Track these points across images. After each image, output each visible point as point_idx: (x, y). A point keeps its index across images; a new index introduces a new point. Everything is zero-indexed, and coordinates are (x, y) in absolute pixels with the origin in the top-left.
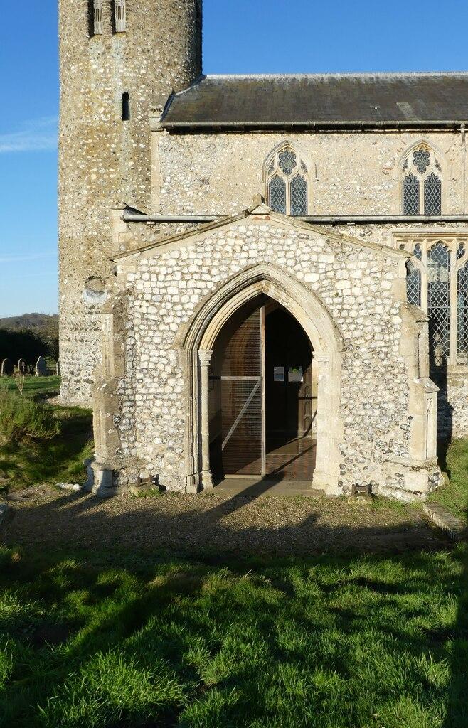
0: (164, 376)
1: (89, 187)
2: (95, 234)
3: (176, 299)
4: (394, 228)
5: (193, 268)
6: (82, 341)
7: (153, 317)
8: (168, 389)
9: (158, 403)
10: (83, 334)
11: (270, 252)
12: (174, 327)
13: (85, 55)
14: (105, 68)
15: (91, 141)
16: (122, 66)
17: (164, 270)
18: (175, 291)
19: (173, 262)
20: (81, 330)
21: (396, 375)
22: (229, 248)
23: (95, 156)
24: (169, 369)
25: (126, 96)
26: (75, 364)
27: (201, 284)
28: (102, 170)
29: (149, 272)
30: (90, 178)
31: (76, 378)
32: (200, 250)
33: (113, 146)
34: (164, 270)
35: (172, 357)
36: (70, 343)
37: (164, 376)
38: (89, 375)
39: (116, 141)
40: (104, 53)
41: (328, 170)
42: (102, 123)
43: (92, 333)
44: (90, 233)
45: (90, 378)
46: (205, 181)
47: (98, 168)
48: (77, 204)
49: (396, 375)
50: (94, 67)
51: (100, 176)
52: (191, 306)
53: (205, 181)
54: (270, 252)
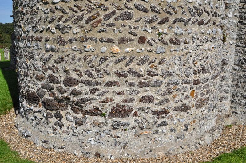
6: (175, 42)
10: (180, 29)
20: (174, 22)
26: (157, 84)
31: (159, 108)
36: (145, 47)
43: (195, 29)
45: (186, 102)
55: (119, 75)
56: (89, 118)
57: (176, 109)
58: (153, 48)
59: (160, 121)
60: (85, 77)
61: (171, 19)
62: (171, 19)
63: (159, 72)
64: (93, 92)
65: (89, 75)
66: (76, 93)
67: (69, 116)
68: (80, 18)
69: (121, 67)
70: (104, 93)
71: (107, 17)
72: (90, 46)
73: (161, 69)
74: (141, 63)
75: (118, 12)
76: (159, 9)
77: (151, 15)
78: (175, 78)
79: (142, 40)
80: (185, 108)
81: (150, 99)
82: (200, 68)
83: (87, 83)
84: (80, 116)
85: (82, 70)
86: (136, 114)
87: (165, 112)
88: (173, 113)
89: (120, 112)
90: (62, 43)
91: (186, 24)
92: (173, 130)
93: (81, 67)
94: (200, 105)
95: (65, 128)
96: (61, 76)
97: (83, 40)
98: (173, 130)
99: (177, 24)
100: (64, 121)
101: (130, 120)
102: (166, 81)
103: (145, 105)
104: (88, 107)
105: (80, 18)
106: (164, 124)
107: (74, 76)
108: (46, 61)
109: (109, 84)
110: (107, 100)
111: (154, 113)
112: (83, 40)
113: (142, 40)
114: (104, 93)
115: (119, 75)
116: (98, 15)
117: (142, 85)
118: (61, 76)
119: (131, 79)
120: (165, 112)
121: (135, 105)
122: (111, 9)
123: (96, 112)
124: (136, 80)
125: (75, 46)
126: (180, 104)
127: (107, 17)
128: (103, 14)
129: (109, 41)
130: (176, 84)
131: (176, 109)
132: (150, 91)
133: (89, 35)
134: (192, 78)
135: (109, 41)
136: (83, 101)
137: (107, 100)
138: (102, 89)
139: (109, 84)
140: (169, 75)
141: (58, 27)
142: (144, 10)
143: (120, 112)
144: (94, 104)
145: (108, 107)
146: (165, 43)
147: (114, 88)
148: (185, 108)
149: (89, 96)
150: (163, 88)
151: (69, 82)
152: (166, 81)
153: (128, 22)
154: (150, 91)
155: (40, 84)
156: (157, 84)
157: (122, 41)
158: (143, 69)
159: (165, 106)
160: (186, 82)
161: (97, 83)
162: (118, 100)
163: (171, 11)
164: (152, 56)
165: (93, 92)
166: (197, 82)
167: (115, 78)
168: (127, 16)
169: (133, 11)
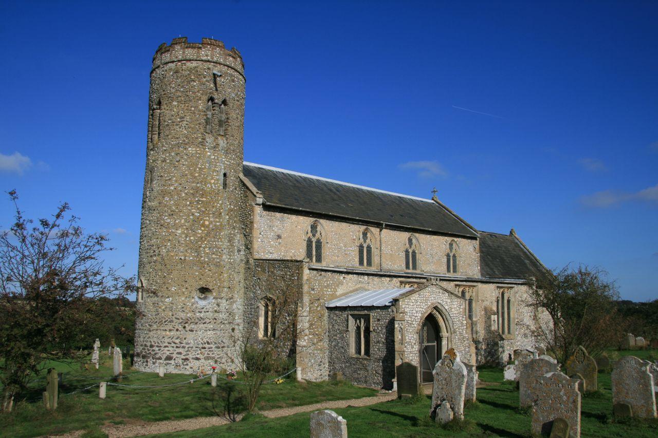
0: (413, 344)
1: (202, 229)
2: (207, 260)
3: (415, 315)
4: (400, 279)
5: (419, 303)
6: (192, 331)
7: (410, 322)
8: (414, 349)
9: (411, 355)
10: (193, 326)
11: (436, 298)
12: (415, 326)
13: (202, 145)
14: (215, 156)
15: (204, 199)
16: (223, 157)
17: (412, 304)
18: (414, 312)
19: (413, 301)
21: (465, 341)
22: (427, 296)
23: (208, 209)
24: (414, 342)
25: (225, 175)
27: (421, 310)
28: (212, 219)
29: (408, 304)
30: (204, 223)
31: (184, 357)
32: (420, 297)
33: (218, 205)
34: (412, 304)
35: (415, 337)
36: (178, 333)
37: (413, 344)
38: (198, 354)
39: (220, 202)
40: (215, 147)
41: (332, 237)
42: (213, 189)
44: (202, 259)
45: (198, 356)
46: (279, 237)
47: (209, 217)
48: (192, 238)
49: (465, 341)
50: (209, 154)
51: (211, 223)
52: (419, 317)
53: (279, 237)
54: (436, 298)
55: (169, 343)
56: (158, 361)
57: (193, 358)
58: (182, 333)
59: (185, 363)
60: (157, 344)
61: (189, 322)
62: (189, 322)
63: (184, 342)
64: (159, 350)
65: (158, 343)
66: (153, 351)
67: (150, 361)
68: (156, 322)
69: (170, 340)
70: (163, 350)
71: (165, 322)
72: (159, 332)
73: (185, 341)
74: (177, 339)
75: (169, 320)
76: (184, 318)
77: (181, 321)
78: (191, 345)
79: (177, 330)
80: (198, 359)
81: (180, 353)
82: (205, 342)
83: (157, 346)
84: (154, 361)
85: (156, 341)
86: (175, 360)
87: (187, 359)
88: (192, 360)
89: (169, 358)
90: (150, 331)
91: (196, 323)
92: (191, 368)
93: (155, 340)
95: (148, 366)
96: (149, 344)
97: (157, 330)
98: (191, 368)
99: (192, 324)
100: (149, 364)
101: (172, 362)
102: (187, 346)
103: (179, 356)
104: (157, 356)
105: (156, 322)
106: (187, 365)
107: (153, 344)
108: (144, 338)
109: (165, 347)
110: (164, 353)
111: (182, 359)
112: (157, 330)
113: (177, 330)
114: (163, 350)
115: (169, 343)
116: (162, 321)
117: (177, 347)
118: (149, 344)
119: (173, 345)
120: (187, 359)
121: (174, 356)
122: (167, 319)
123: (160, 358)
124: (175, 345)
125: (154, 332)
126: (194, 356)
127: (165, 322)
128: (164, 321)
129: (166, 330)
130: (192, 347)
131: (193, 358)
132: (180, 350)
133: (159, 328)
134: (201, 346)
135: (166, 330)
136: (156, 354)
137: (164, 353)
138: (162, 349)
139: (165, 347)
140: (189, 344)
141: (149, 325)
142: (178, 319)
143: (169, 358)
144: (159, 355)
145: (165, 356)
146: (187, 331)
147: (167, 349)
148: (198, 359)
149: (158, 352)
150: (186, 349)
151: (152, 346)
152: (187, 346)
153: (172, 324)
154: (180, 350)
155: (142, 348)
156: (184, 347)
157: (170, 330)
158: (177, 341)
159: (187, 357)
160: (197, 347)
161: (161, 347)
162: (168, 353)
163: (189, 319)
164: (181, 336)
165: (159, 350)
166: (204, 348)
167: (167, 345)
168: (172, 321)
169: (174, 319)
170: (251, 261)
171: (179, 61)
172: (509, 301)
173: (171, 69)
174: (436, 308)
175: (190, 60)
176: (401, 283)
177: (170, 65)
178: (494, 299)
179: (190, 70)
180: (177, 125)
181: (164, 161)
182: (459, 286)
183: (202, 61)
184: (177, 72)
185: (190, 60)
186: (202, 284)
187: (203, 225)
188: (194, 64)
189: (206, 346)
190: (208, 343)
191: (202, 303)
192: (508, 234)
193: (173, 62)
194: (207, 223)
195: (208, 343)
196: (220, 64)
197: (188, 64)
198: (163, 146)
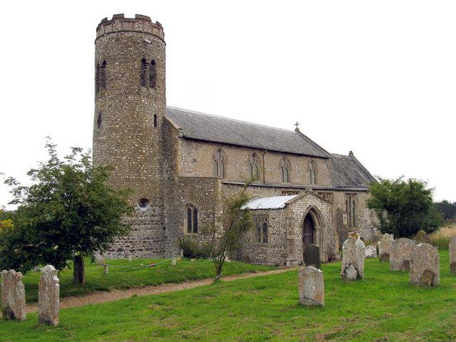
4: (282, 190)
6: (136, 230)
10: (137, 227)
25: (155, 115)
43: (143, 226)
53: (195, 161)
80: (141, 250)
81: (128, 246)
89: (120, 250)
94: (146, 250)
101: (123, 253)
119: (122, 240)
121: (124, 248)
123: (113, 250)
132: (128, 244)
143: (120, 250)
145: (116, 249)
148: (141, 250)
154: (128, 244)
162: (119, 247)
170: (176, 179)
171: (119, 32)
172: (354, 203)
173: (112, 38)
174: (312, 209)
175: (127, 31)
176: (283, 192)
177: (112, 35)
178: (344, 202)
179: (128, 38)
180: (120, 79)
181: (110, 106)
182: (321, 193)
183: (136, 31)
184: (117, 40)
185: (127, 31)
186: (142, 196)
187: (141, 153)
188: (130, 34)
189: (147, 240)
190: (148, 238)
191: (143, 209)
192: (348, 154)
193: (114, 32)
194: (144, 151)
195: (148, 238)
196: (149, 34)
197: (126, 34)
198: (109, 95)
